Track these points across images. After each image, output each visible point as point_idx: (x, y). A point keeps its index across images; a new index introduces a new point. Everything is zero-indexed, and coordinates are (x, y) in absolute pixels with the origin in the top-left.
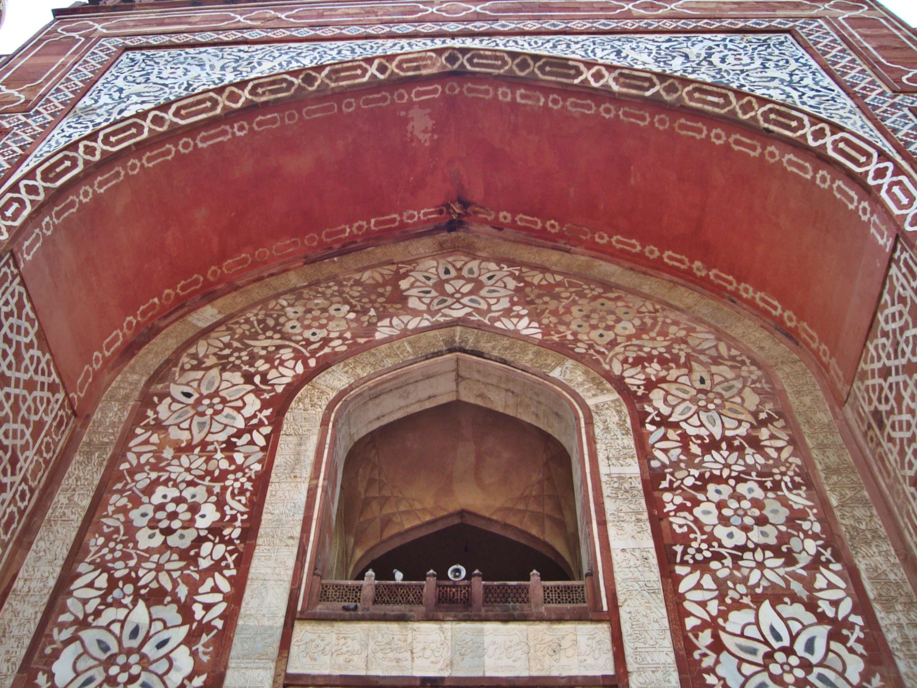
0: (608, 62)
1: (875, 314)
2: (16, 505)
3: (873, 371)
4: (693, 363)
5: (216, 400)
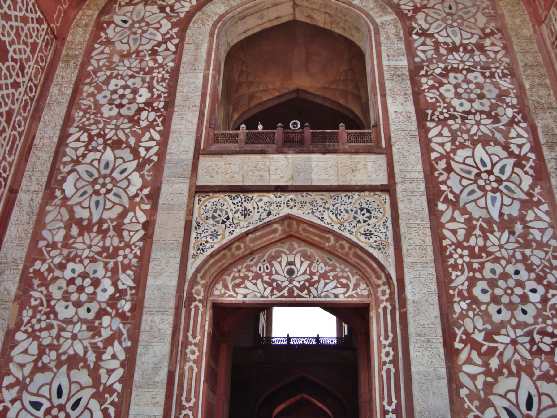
2: (28, 95)
5: (143, 24)
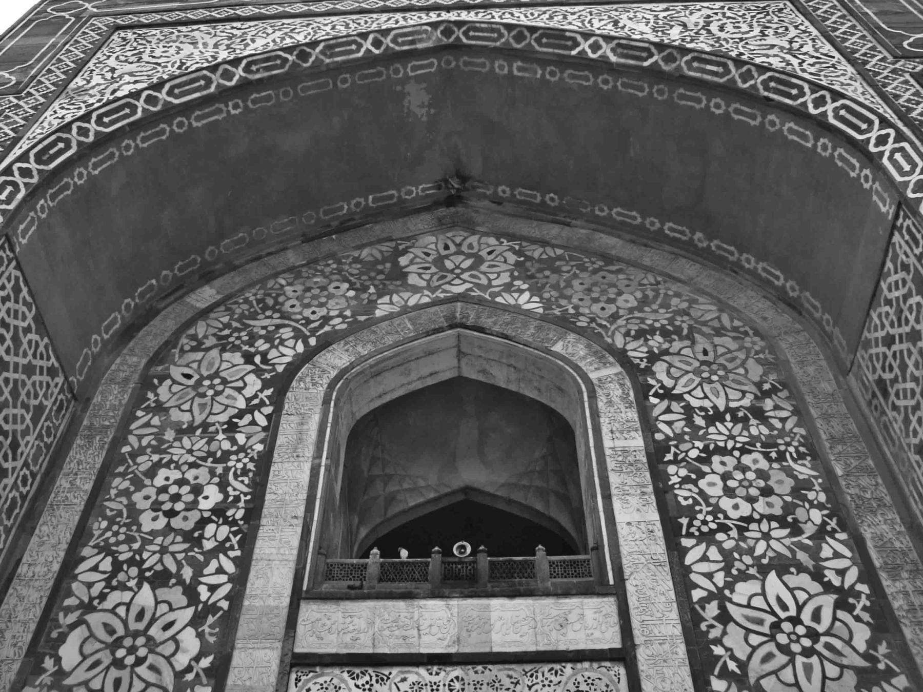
0: (605, 32)
1: (878, 284)
2: (17, 490)
3: (877, 339)
4: (696, 335)
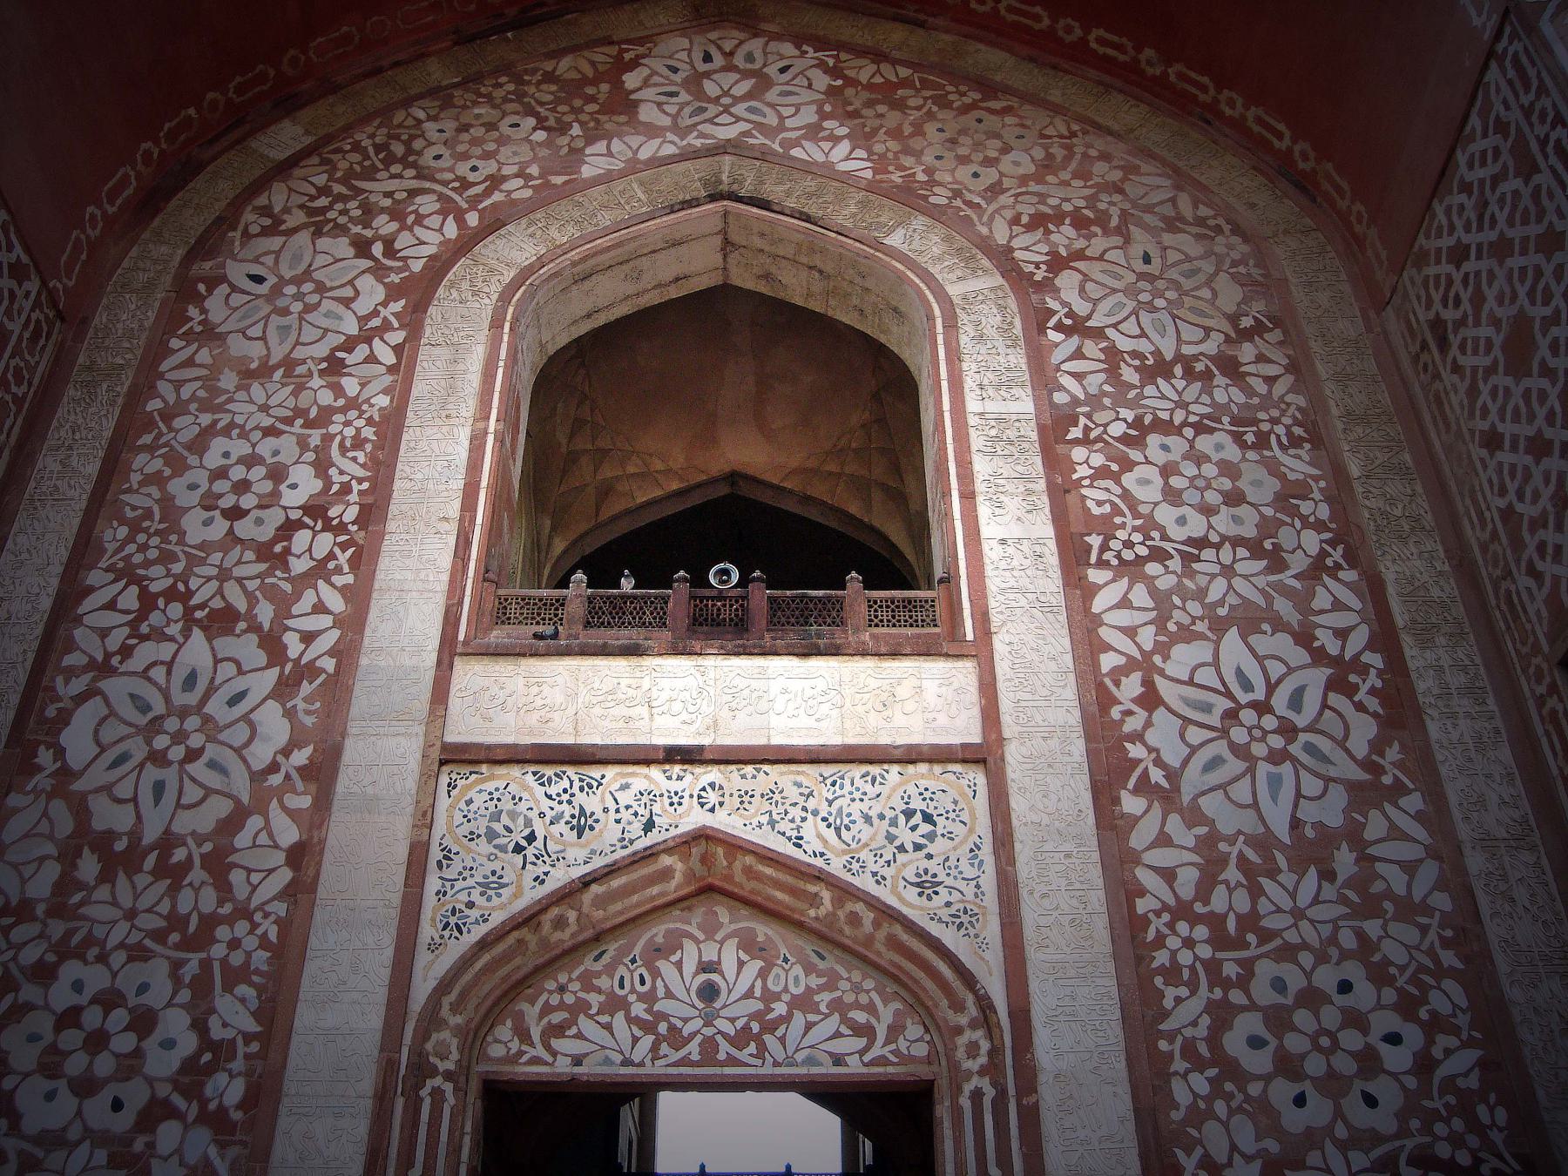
1: (1452, 151)
4: (1132, 227)
5: (308, 287)
